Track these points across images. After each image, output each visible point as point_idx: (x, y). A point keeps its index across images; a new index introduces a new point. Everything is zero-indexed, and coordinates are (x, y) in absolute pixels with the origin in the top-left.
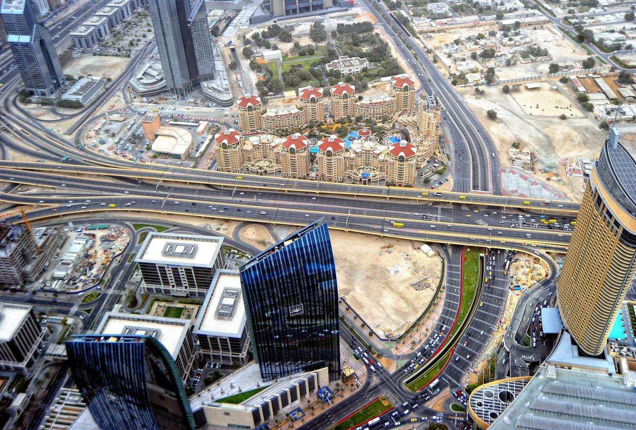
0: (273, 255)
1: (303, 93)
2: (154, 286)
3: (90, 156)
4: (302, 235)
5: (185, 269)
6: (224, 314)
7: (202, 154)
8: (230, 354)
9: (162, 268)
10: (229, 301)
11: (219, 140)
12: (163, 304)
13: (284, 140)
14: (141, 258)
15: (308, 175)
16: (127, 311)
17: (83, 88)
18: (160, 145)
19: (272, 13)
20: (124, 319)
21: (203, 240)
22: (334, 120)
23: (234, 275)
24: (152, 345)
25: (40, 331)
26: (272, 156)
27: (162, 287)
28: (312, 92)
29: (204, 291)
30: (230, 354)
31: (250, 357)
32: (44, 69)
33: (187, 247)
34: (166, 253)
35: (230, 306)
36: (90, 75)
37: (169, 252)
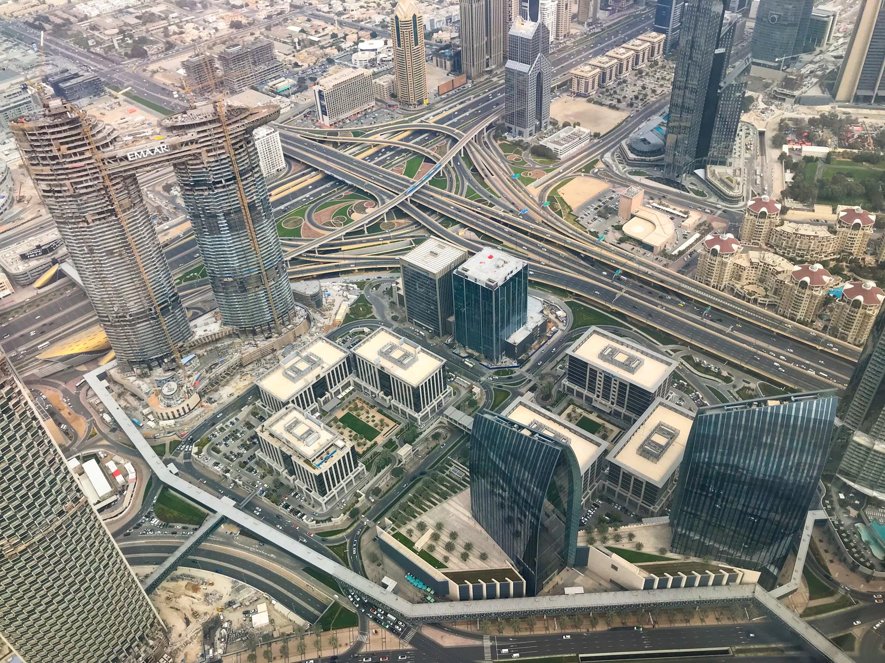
0: (748, 412)
1: (845, 213)
2: (576, 388)
3: (550, 217)
4: (796, 401)
5: (620, 383)
6: (651, 452)
7: (681, 253)
8: (640, 501)
9: (594, 372)
10: (661, 440)
11: (711, 243)
12: (579, 411)
13: (797, 268)
14: (574, 351)
15: (813, 321)
16: (538, 403)
17: (567, 139)
18: (633, 228)
19: (834, 96)
20: (535, 411)
21: (652, 357)
22: (877, 261)
23: (687, 416)
24: (565, 457)
25: (445, 388)
26: (771, 281)
27: (585, 392)
28: (859, 216)
29: (633, 416)
30: (640, 501)
31: (662, 513)
32: (531, 105)
33: (631, 359)
34: (602, 356)
35: (660, 446)
36: (579, 124)
37: (608, 356)
